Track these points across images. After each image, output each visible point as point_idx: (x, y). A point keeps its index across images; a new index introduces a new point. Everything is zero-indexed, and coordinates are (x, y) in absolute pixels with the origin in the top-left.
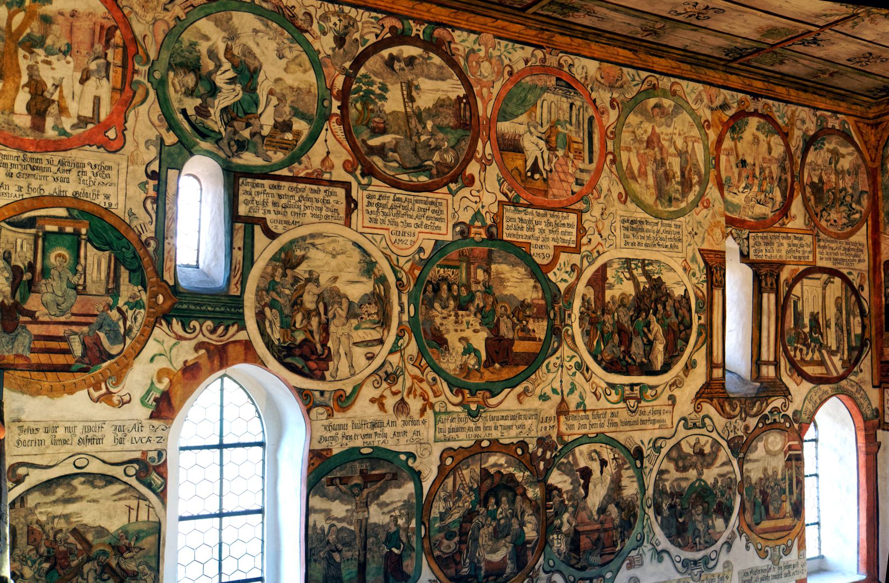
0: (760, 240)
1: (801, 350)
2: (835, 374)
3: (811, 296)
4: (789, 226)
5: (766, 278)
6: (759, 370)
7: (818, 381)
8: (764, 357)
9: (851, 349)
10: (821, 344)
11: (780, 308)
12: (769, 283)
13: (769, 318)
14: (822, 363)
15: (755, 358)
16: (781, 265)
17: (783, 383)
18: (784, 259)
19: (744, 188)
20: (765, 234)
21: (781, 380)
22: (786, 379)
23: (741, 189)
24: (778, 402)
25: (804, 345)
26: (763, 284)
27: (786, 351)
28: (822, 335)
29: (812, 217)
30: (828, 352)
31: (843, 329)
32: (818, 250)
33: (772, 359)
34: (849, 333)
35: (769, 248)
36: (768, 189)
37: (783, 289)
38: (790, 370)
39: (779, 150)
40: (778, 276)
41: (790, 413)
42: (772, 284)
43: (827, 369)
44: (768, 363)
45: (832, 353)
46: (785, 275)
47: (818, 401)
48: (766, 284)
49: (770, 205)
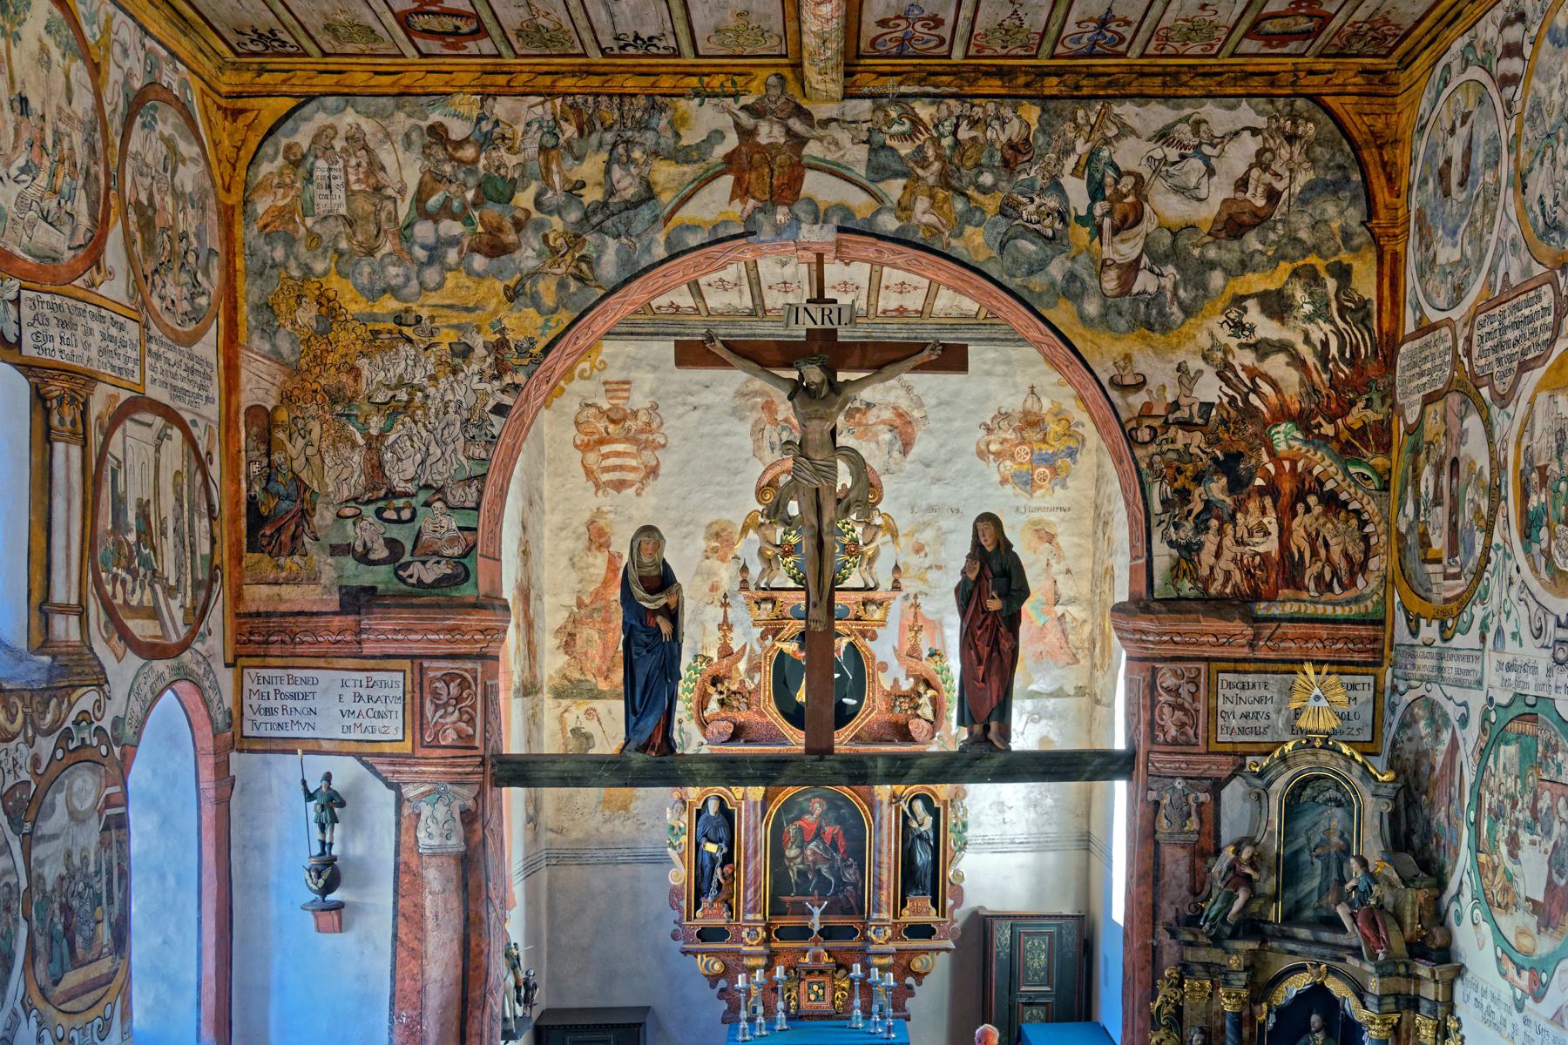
0: (47, 311)
1: (124, 582)
2: (174, 639)
3: (144, 462)
4: (101, 290)
5: (60, 405)
6: (47, 626)
7: (152, 651)
8: (59, 595)
9: (197, 585)
10: (154, 571)
11: (89, 482)
12: (68, 419)
13: (69, 502)
14: (154, 613)
15: (37, 596)
16: (92, 379)
17: (96, 657)
18: (95, 368)
19: (22, 170)
20: (58, 300)
21: (91, 649)
22: (100, 648)
23: (14, 172)
24: (86, 700)
25: (128, 570)
26: (55, 420)
27: (98, 583)
28: (154, 549)
29: (141, 282)
30: (164, 588)
31: (186, 543)
32: (148, 360)
33: (74, 600)
34: (193, 553)
35: (67, 334)
36: (66, 189)
37: (96, 438)
38: (106, 627)
39: (83, 102)
40: (86, 404)
41: (106, 724)
42: (73, 423)
43: (163, 626)
44: (65, 609)
45: (171, 592)
46: (98, 405)
47: (150, 696)
48: (62, 420)
49: (67, 230)
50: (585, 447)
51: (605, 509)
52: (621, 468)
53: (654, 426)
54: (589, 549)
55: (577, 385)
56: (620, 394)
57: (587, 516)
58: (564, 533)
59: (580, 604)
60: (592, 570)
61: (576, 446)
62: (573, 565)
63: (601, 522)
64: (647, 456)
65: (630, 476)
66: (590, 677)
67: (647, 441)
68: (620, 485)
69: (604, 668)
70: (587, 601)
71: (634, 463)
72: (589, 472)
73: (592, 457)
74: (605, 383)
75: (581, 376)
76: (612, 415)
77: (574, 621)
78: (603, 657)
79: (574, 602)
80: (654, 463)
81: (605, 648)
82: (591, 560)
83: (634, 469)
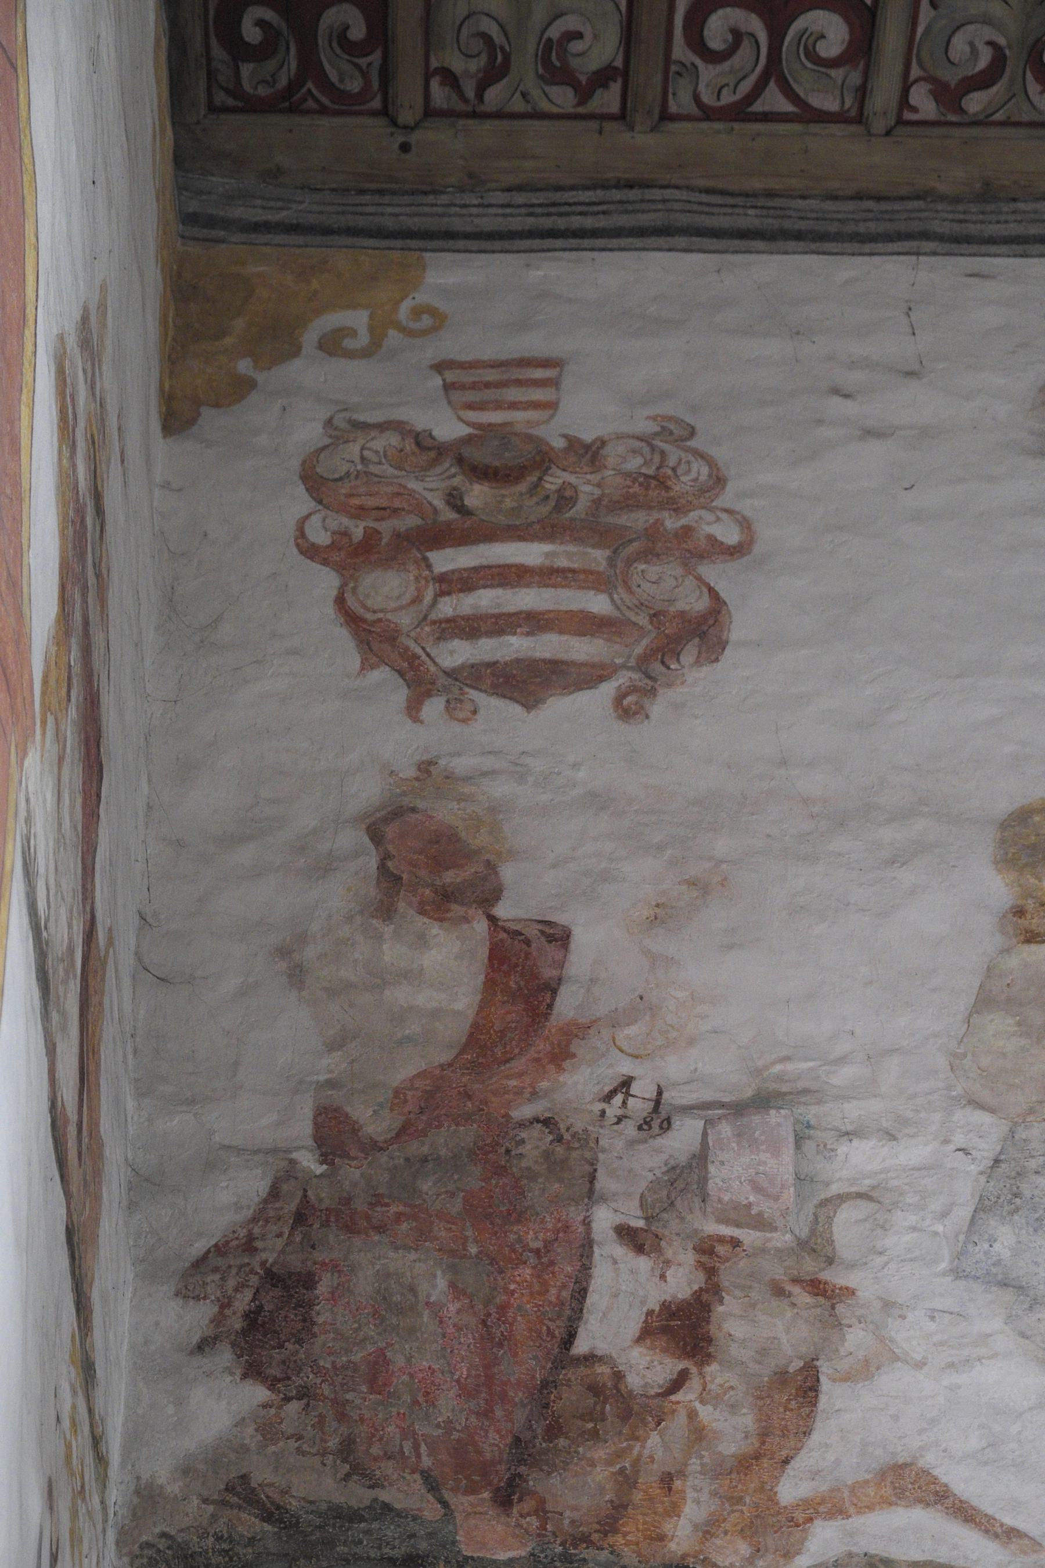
50: (352, 556)
51: (462, 765)
52: (535, 622)
53: (683, 486)
54: (385, 911)
55: (309, 371)
56: (513, 394)
57: (368, 792)
58: (245, 855)
59: (333, 1133)
60: (400, 995)
61: (310, 551)
62: (297, 976)
63: (447, 813)
64: (665, 583)
65: (582, 649)
66: (405, 1493)
67: (653, 533)
68: (524, 684)
69: (493, 1443)
70: (373, 1120)
71: (598, 604)
72: (372, 637)
73: (386, 589)
74: (440, 367)
75: (332, 345)
76: (472, 453)
77: (299, 1210)
78: (485, 1389)
79: (302, 1128)
80: (697, 603)
81: (493, 1337)
82: (393, 953)
83: (587, 625)
